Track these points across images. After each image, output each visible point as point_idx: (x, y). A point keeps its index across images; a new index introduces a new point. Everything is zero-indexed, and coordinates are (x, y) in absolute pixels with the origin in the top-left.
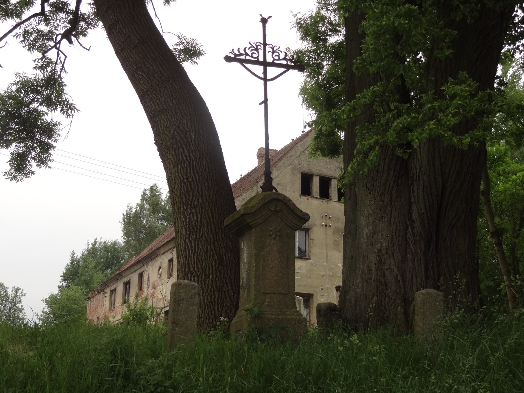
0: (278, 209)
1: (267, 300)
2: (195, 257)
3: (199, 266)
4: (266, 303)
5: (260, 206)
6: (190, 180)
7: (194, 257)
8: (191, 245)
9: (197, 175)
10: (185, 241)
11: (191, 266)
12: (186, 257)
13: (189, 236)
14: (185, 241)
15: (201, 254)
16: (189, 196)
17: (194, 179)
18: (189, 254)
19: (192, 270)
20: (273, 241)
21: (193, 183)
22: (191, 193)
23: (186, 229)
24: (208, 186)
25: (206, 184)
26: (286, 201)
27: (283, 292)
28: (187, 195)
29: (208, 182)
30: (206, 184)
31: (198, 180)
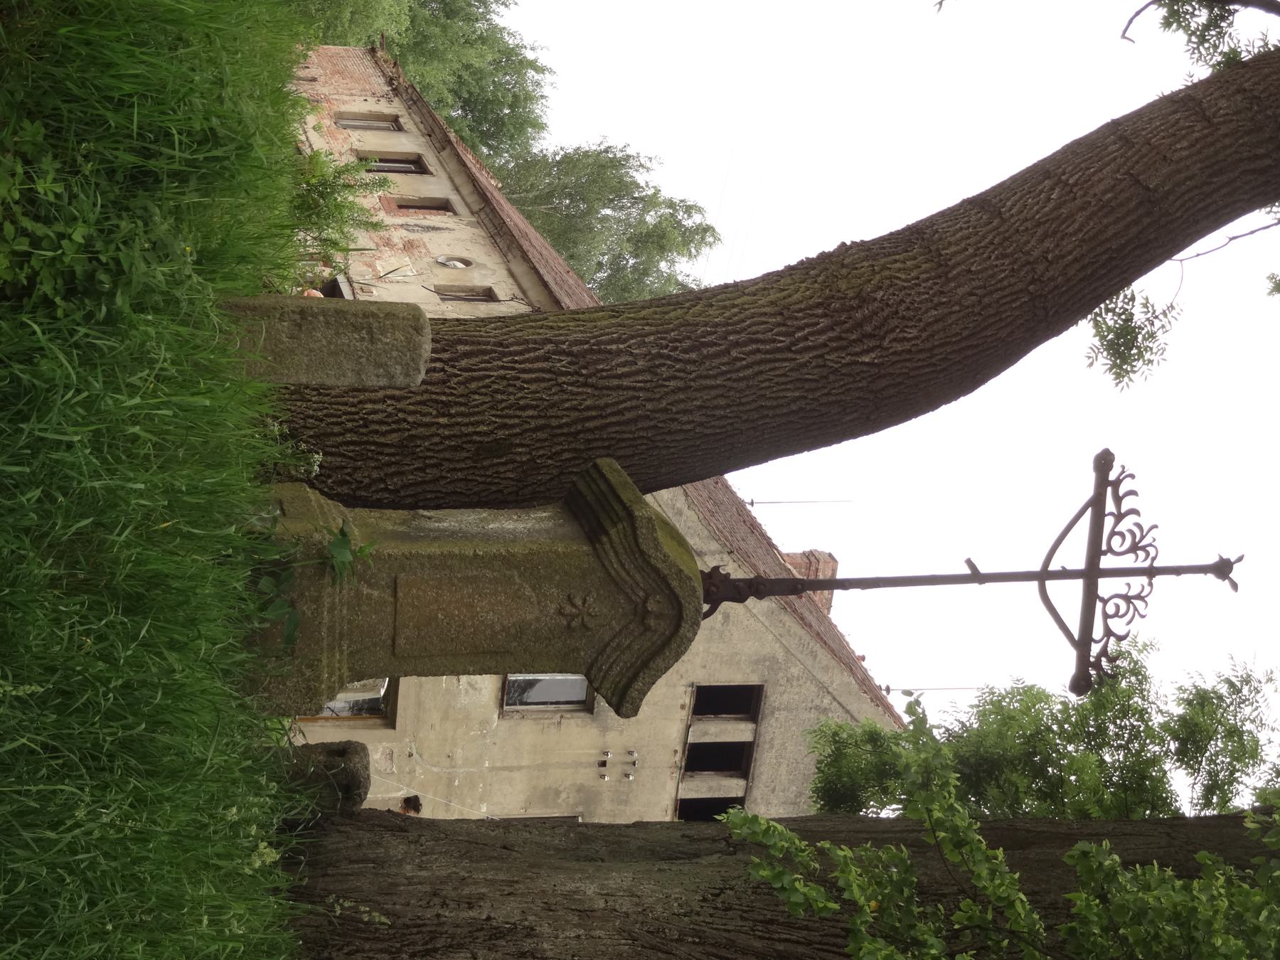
0: (652, 622)
1: (376, 593)
2: (502, 372)
3: (473, 386)
4: (366, 590)
5: (659, 566)
6: (734, 353)
7: (502, 367)
8: (537, 359)
9: (749, 372)
10: (550, 341)
11: (474, 360)
12: (501, 345)
13: (563, 352)
14: (550, 341)
15: (511, 389)
16: (685, 351)
17: (739, 364)
18: (511, 354)
19: (463, 363)
20: (552, 608)
21: (725, 359)
22: (693, 356)
23: (587, 342)
24: (716, 407)
25: (722, 402)
26: (674, 646)
27: (401, 641)
28: (688, 343)
29: (729, 406)
30: (722, 402)
31: (734, 376)
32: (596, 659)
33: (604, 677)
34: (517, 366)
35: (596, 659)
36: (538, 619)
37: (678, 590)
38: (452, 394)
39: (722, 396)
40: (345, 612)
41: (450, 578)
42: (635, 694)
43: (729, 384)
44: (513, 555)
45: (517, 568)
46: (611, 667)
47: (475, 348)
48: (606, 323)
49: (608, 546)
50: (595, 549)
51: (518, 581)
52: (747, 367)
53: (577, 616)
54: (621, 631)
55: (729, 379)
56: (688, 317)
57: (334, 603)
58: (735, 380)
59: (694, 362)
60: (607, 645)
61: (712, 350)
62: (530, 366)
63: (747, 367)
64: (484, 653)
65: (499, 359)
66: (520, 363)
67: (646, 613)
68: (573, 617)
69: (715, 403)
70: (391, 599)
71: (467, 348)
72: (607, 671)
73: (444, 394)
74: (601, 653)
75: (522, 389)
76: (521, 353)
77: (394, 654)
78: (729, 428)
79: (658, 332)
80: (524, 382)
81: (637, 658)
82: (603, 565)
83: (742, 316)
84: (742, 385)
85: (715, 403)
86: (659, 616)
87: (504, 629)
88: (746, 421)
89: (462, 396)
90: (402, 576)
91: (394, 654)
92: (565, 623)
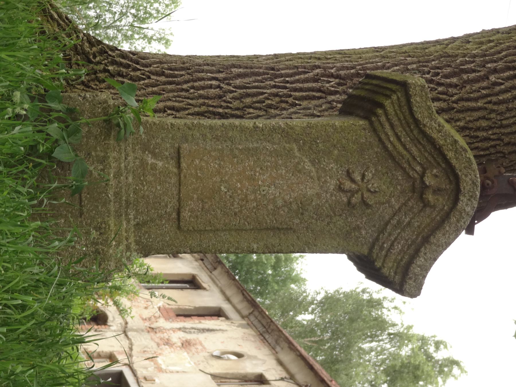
0: (430, 197)
1: (160, 164)
2: (274, 90)
3: (248, 100)
4: (150, 160)
5: (435, 135)
6: (493, 78)
7: (275, 87)
8: (307, 81)
9: (508, 95)
10: (318, 67)
11: (247, 80)
12: (273, 69)
13: (332, 76)
14: (318, 67)
15: (284, 105)
16: (446, 76)
17: (498, 88)
18: (281, 76)
19: (238, 82)
20: (332, 184)
21: (485, 84)
22: (454, 80)
23: (353, 68)
24: (478, 129)
25: (484, 123)
26: (453, 220)
27: (186, 214)
28: (449, 70)
29: (491, 128)
30: (484, 123)
31: (494, 99)
32: (377, 239)
33: (386, 256)
34: (288, 85)
35: (377, 239)
36: (318, 195)
37: (454, 162)
38: (228, 107)
39: (484, 118)
40: (130, 179)
41: (232, 150)
42: (417, 270)
43: (490, 106)
44: (292, 128)
45: (296, 141)
46: (392, 245)
47: (249, 70)
48: (370, 55)
49: (383, 119)
50: (371, 123)
51: (297, 154)
52: (506, 91)
53: (357, 192)
54: (400, 209)
55: (490, 102)
56: (446, 50)
57: (120, 168)
58: (495, 103)
59: (456, 86)
60: (387, 223)
61: (472, 76)
62: (301, 85)
63: (506, 91)
64: (267, 229)
65: (272, 80)
66: (292, 83)
67: (425, 187)
68: (353, 193)
69: (478, 124)
70: (175, 170)
71: (241, 70)
72: (389, 250)
73: (221, 107)
74: (382, 231)
75: (294, 105)
76: (291, 75)
77: (179, 227)
78: (492, 150)
79: (419, 62)
80: (296, 99)
81: (418, 236)
82: (380, 140)
83: (498, 48)
84: (502, 108)
85: (478, 124)
86: (437, 191)
87: (287, 204)
88: (509, 144)
89: (238, 109)
90: (185, 146)
91: (179, 227)
92: (345, 199)
